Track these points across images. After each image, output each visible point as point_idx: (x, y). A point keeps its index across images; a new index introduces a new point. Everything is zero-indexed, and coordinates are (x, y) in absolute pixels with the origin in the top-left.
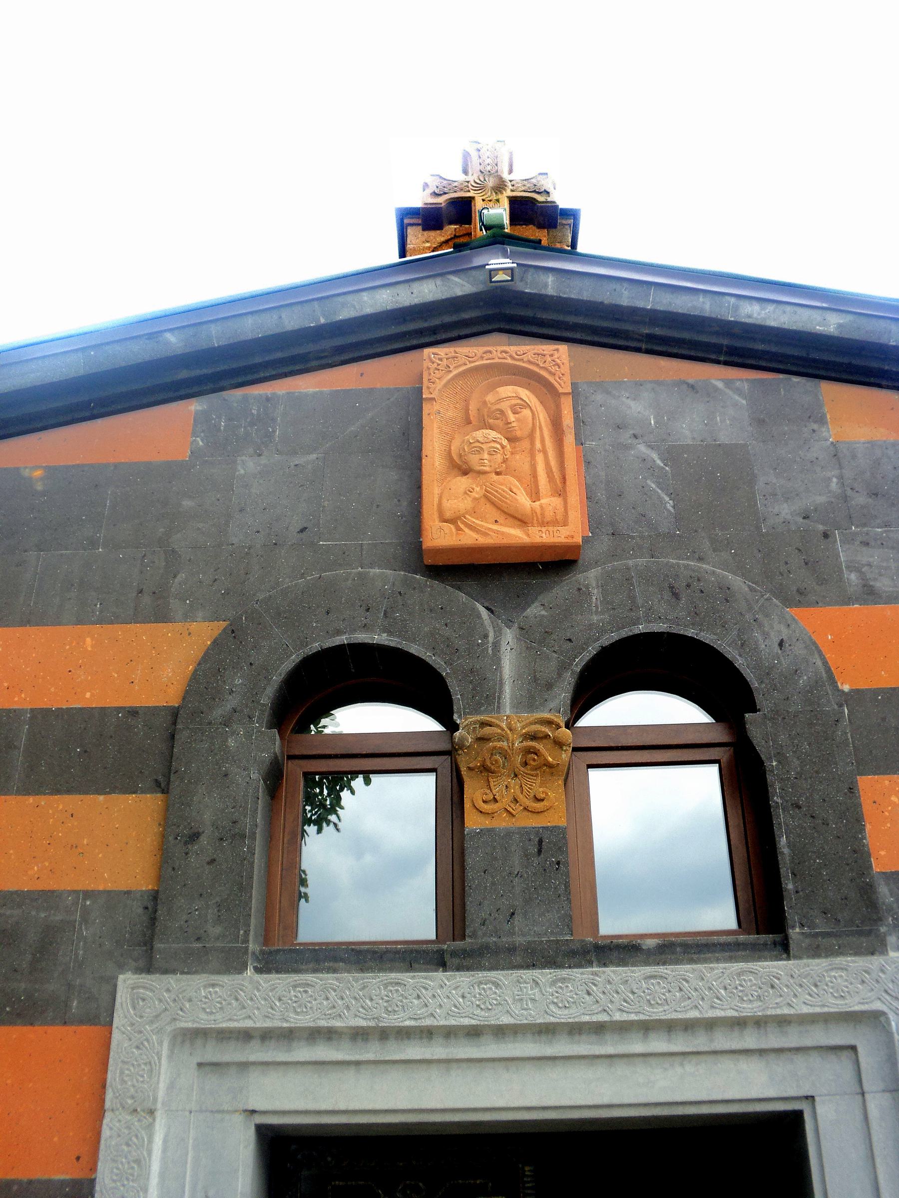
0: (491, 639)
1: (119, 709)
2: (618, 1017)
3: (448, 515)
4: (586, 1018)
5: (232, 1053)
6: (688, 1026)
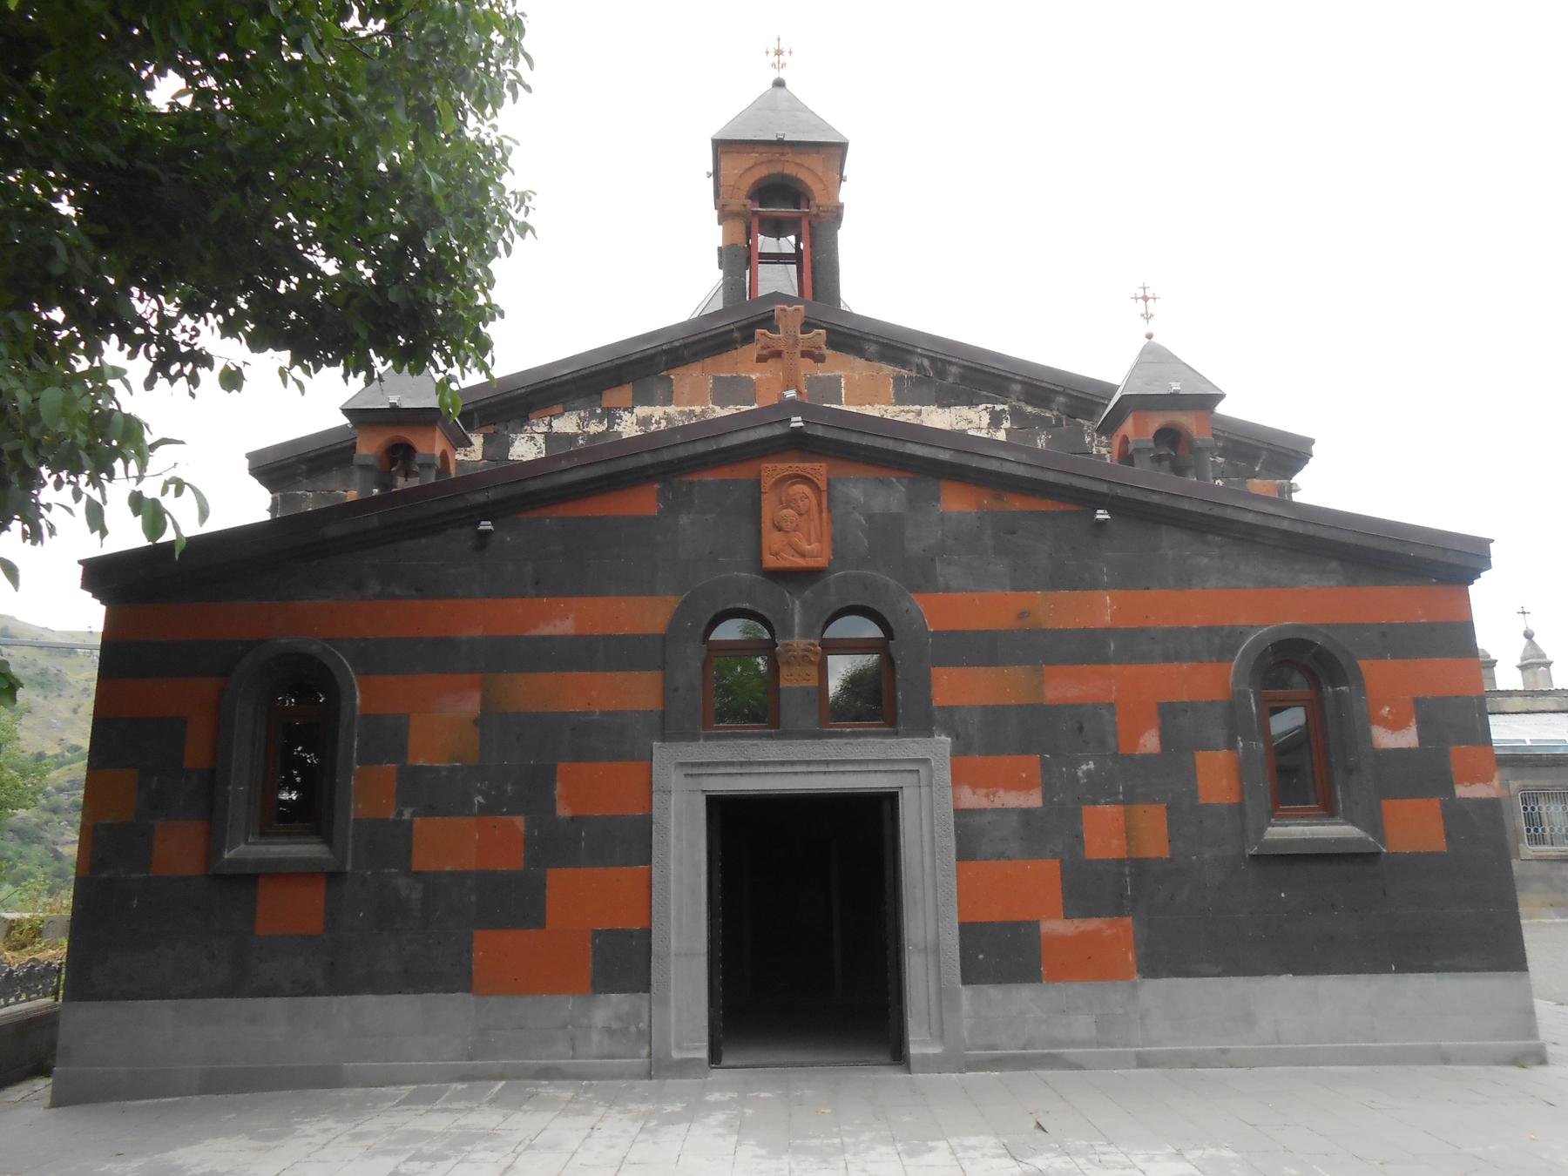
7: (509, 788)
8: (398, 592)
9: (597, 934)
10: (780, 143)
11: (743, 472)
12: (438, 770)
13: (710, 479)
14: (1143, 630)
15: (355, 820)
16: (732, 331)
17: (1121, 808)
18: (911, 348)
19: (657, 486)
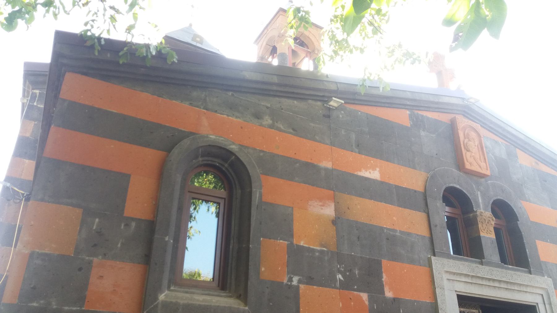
7: (357, 272)
12: (313, 251)
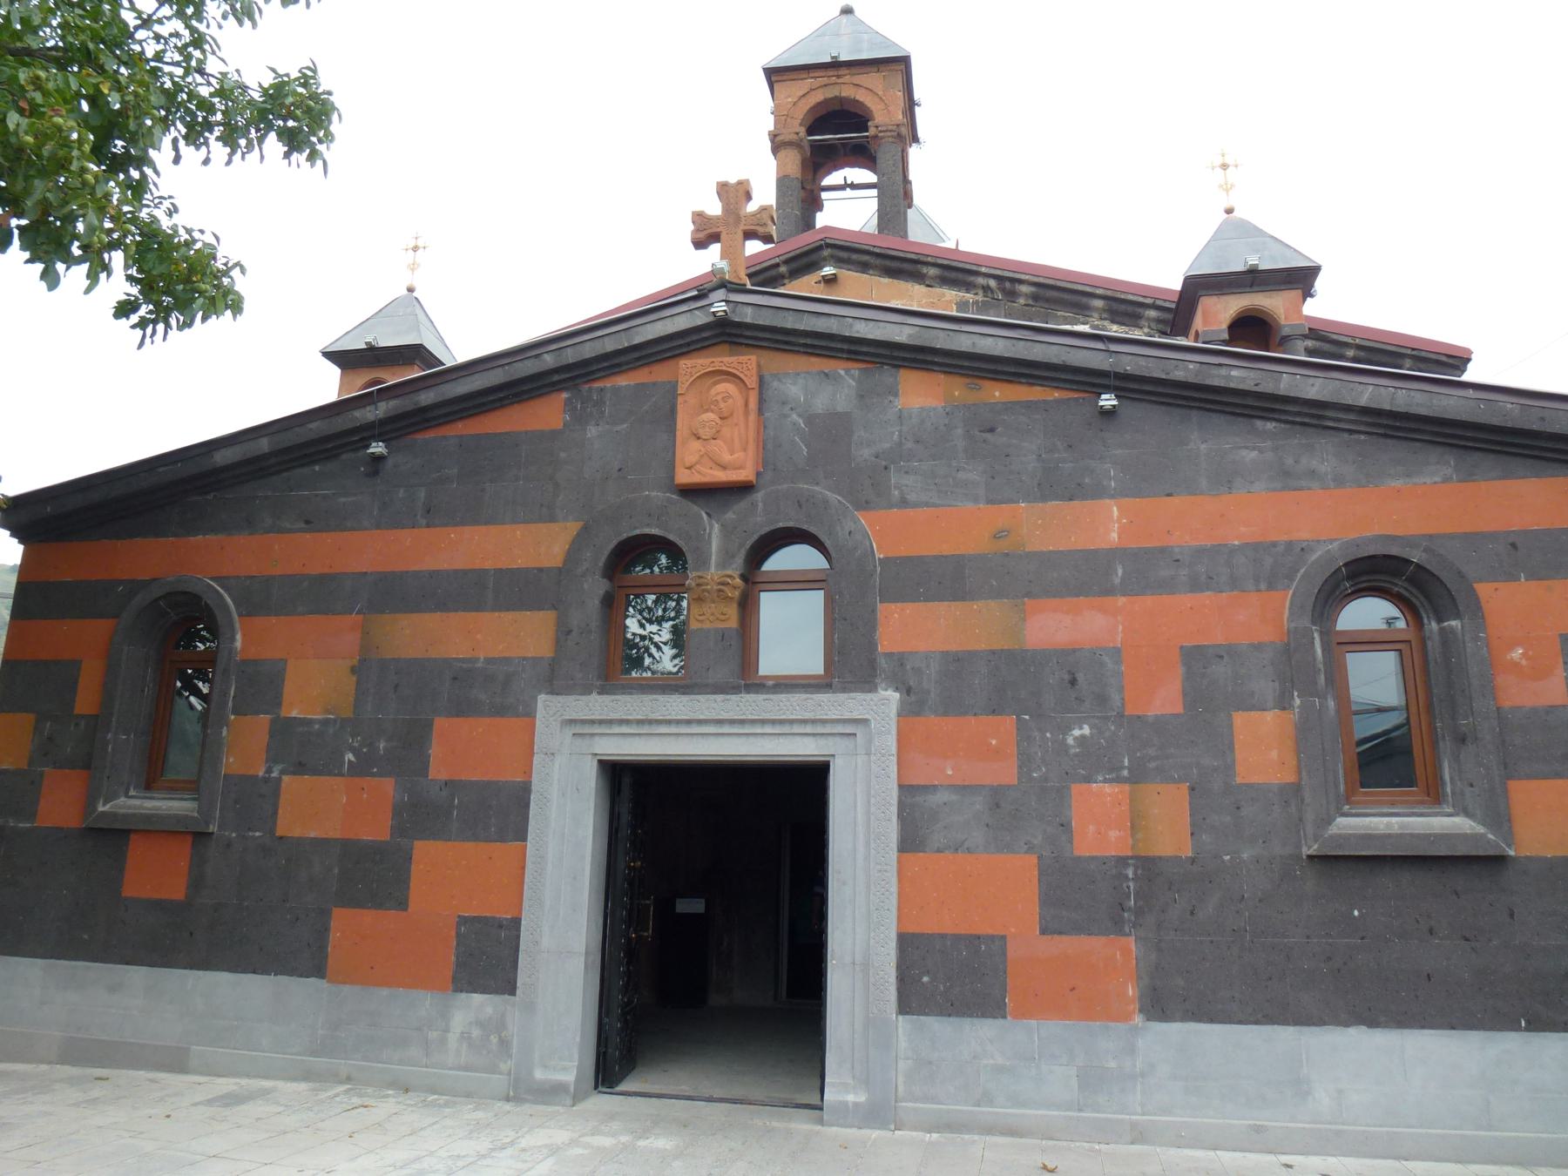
0: (708, 531)
1: (534, 568)
2: (750, 717)
3: (688, 465)
4: (736, 717)
5: (587, 729)
6: (782, 722)
8: (288, 526)
9: (463, 921)
10: (835, 65)
11: (658, 374)
12: (310, 722)
13: (624, 383)
14: (1163, 551)
15: (225, 775)
16: (777, 265)
17: (1127, 787)
18: (974, 268)
19: (565, 395)
